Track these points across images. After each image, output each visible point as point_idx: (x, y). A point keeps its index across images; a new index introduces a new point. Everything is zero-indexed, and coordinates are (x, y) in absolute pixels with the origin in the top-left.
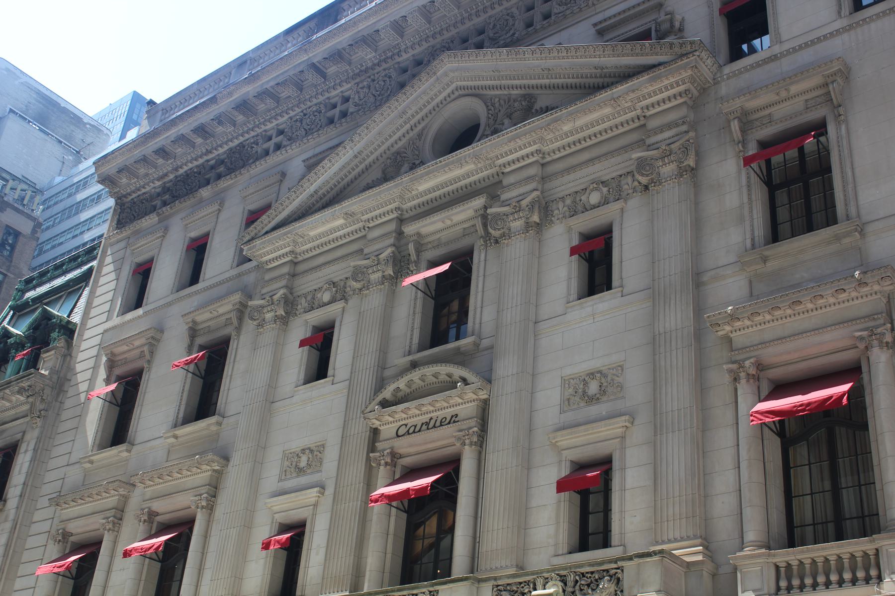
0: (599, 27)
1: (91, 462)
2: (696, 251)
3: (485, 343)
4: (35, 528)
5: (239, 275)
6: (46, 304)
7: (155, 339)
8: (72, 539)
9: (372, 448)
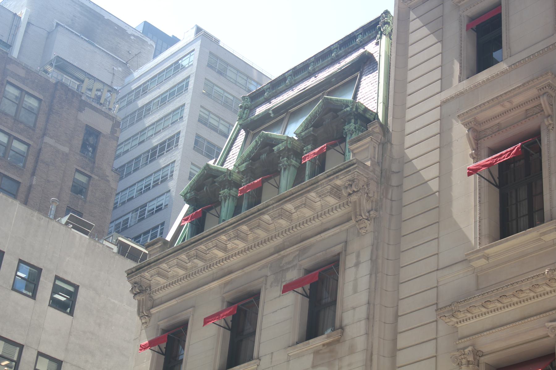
1: (487, 258)
6: (265, 129)
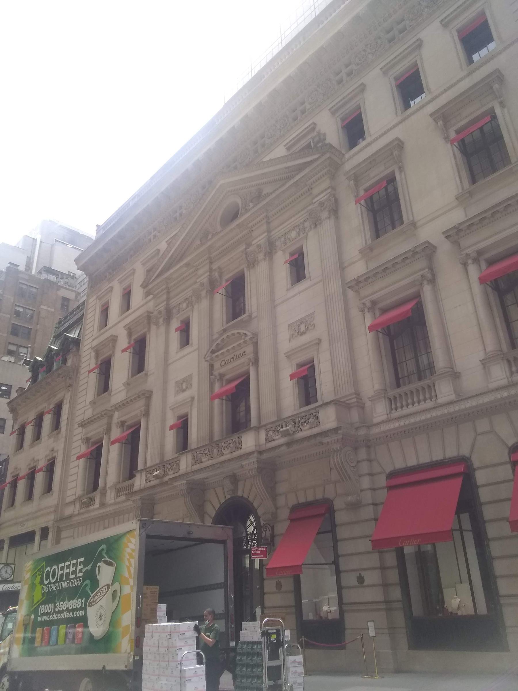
0: (287, 146)
2: (340, 252)
3: (254, 315)
4: (75, 439)
5: (146, 303)
7: (114, 339)
8: (91, 441)
9: (211, 374)
